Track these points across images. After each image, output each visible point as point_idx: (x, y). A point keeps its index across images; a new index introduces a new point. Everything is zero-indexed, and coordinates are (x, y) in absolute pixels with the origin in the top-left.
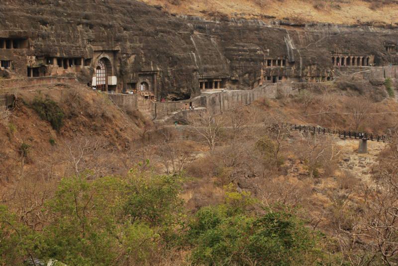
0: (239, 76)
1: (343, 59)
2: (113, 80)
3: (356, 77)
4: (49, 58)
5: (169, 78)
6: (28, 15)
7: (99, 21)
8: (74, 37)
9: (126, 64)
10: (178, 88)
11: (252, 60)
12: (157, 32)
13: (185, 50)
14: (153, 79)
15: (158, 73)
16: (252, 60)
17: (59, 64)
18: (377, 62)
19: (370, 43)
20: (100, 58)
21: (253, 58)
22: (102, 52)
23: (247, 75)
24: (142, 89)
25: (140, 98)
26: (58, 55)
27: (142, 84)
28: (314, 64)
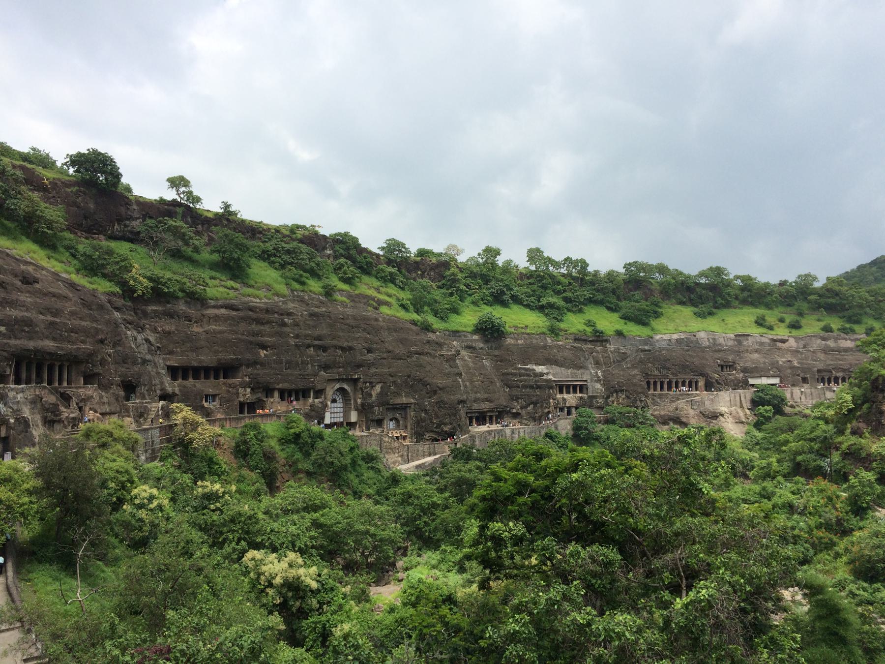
0: (522, 408)
1: (662, 384)
2: (354, 417)
3: (681, 406)
4: (269, 392)
5: (426, 411)
6: (245, 337)
7: (335, 342)
8: (302, 363)
9: (371, 395)
10: (439, 426)
11: (539, 387)
12: (410, 354)
13: (448, 375)
14: (406, 414)
15: (412, 406)
16: (539, 387)
17: (282, 398)
18: (709, 387)
19: (696, 361)
20: (336, 388)
22: (338, 380)
24: (391, 427)
25: (387, 439)
26: (280, 386)
27: (391, 420)
28: (622, 391)
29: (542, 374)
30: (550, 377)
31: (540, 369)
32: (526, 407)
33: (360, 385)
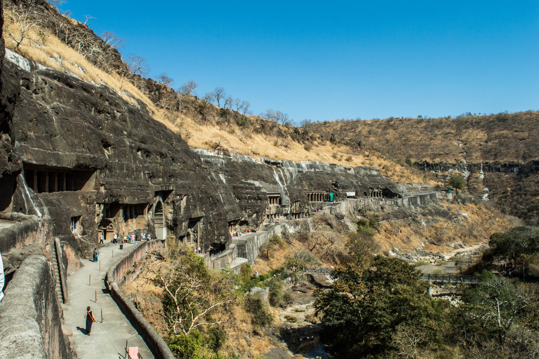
0: (249, 216)
8: (136, 171)
11: (260, 199)
21: (260, 196)
23: (255, 215)
29: (259, 188)
30: (264, 190)
31: (257, 184)
32: (252, 216)
33: (171, 197)
